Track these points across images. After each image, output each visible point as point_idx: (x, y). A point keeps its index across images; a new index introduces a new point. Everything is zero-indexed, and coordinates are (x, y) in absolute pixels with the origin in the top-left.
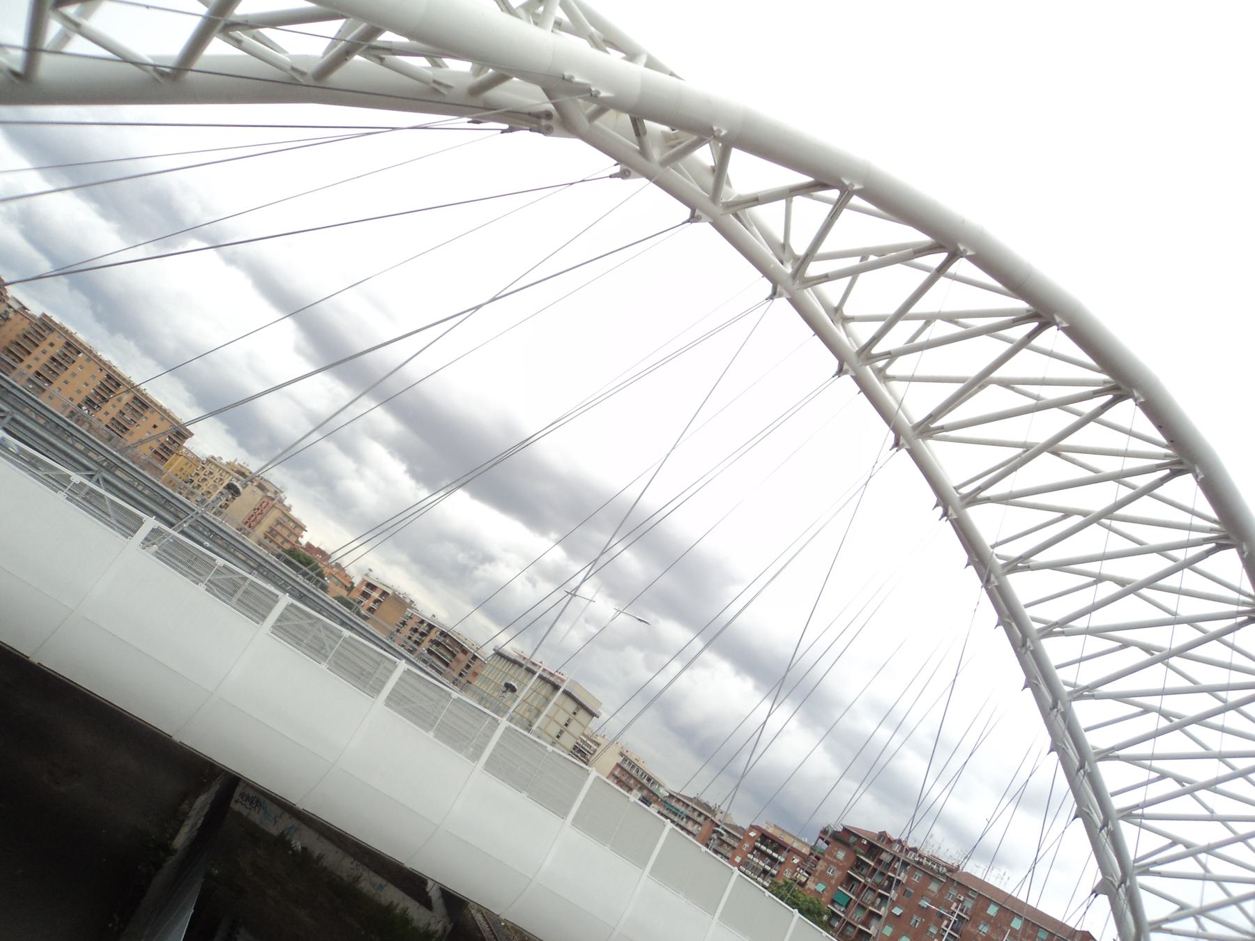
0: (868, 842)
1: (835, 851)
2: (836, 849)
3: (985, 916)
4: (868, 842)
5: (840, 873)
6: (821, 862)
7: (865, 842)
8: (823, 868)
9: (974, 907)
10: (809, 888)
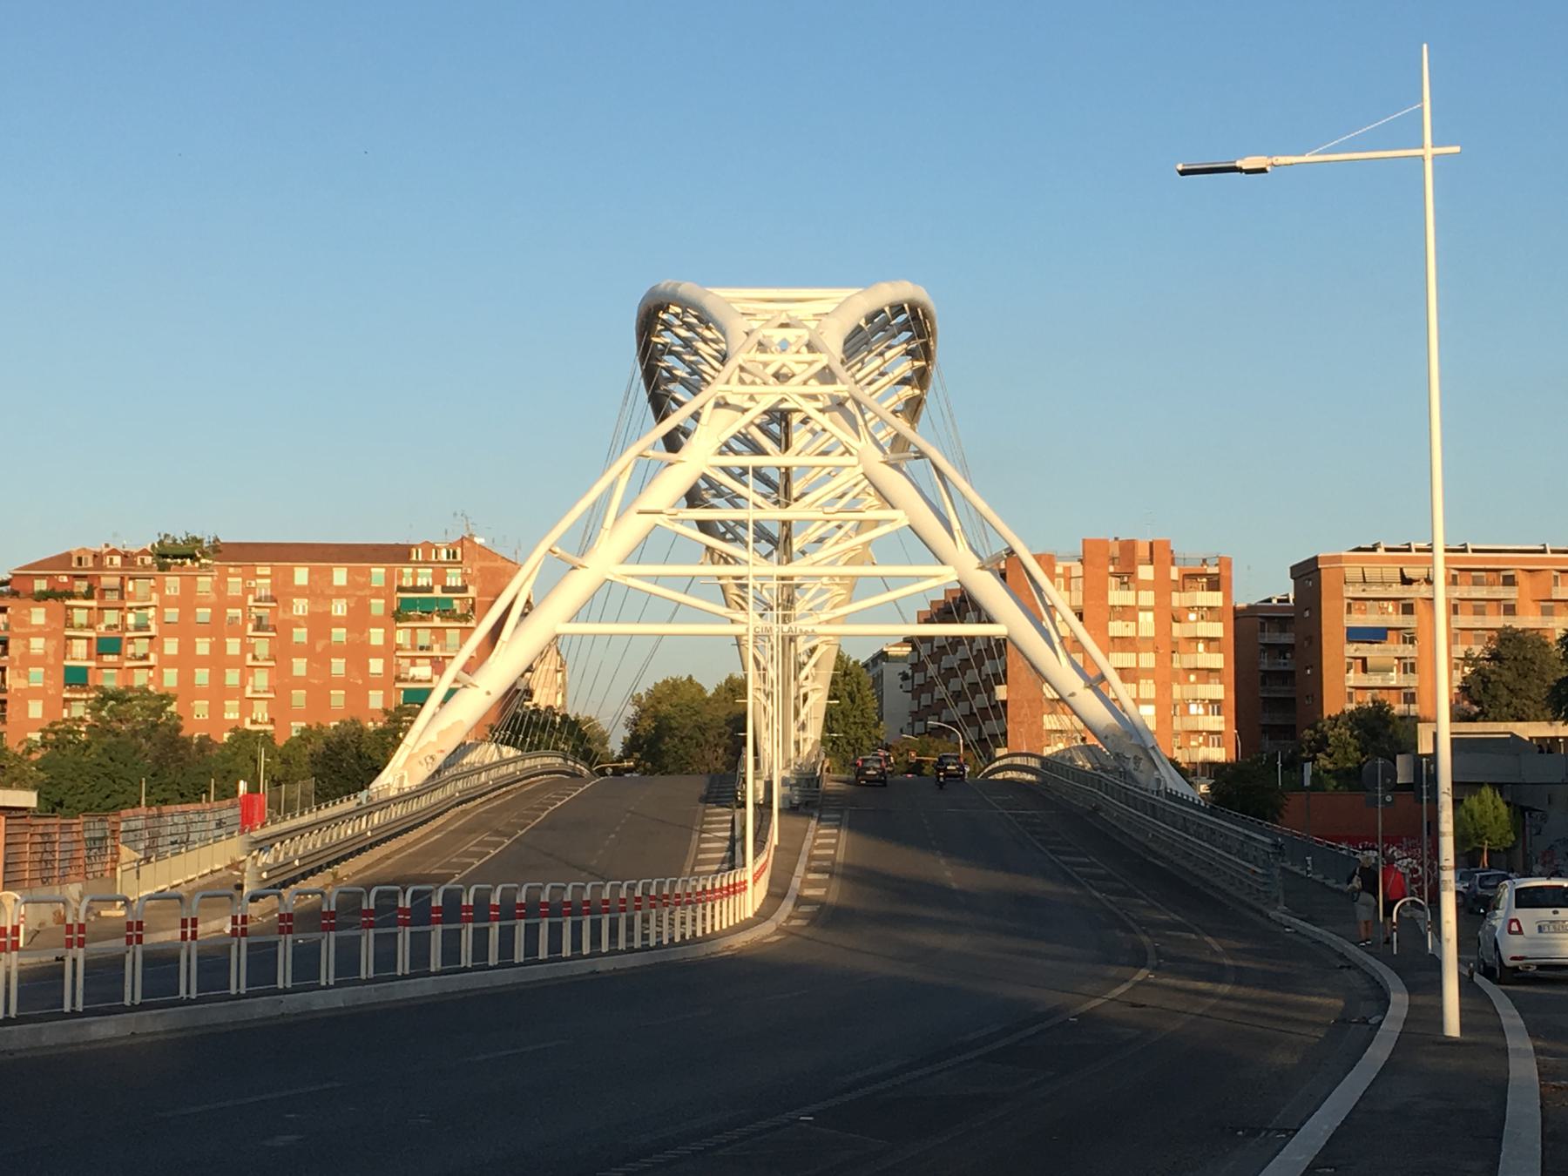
0: (68, 576)
2: (25, 612)
3: (294, 589)
4: (68, 576)
5: (54, 642)
6: (11, 643)
7: (65, 579)
8: (23, 649)
10: (16, 690)
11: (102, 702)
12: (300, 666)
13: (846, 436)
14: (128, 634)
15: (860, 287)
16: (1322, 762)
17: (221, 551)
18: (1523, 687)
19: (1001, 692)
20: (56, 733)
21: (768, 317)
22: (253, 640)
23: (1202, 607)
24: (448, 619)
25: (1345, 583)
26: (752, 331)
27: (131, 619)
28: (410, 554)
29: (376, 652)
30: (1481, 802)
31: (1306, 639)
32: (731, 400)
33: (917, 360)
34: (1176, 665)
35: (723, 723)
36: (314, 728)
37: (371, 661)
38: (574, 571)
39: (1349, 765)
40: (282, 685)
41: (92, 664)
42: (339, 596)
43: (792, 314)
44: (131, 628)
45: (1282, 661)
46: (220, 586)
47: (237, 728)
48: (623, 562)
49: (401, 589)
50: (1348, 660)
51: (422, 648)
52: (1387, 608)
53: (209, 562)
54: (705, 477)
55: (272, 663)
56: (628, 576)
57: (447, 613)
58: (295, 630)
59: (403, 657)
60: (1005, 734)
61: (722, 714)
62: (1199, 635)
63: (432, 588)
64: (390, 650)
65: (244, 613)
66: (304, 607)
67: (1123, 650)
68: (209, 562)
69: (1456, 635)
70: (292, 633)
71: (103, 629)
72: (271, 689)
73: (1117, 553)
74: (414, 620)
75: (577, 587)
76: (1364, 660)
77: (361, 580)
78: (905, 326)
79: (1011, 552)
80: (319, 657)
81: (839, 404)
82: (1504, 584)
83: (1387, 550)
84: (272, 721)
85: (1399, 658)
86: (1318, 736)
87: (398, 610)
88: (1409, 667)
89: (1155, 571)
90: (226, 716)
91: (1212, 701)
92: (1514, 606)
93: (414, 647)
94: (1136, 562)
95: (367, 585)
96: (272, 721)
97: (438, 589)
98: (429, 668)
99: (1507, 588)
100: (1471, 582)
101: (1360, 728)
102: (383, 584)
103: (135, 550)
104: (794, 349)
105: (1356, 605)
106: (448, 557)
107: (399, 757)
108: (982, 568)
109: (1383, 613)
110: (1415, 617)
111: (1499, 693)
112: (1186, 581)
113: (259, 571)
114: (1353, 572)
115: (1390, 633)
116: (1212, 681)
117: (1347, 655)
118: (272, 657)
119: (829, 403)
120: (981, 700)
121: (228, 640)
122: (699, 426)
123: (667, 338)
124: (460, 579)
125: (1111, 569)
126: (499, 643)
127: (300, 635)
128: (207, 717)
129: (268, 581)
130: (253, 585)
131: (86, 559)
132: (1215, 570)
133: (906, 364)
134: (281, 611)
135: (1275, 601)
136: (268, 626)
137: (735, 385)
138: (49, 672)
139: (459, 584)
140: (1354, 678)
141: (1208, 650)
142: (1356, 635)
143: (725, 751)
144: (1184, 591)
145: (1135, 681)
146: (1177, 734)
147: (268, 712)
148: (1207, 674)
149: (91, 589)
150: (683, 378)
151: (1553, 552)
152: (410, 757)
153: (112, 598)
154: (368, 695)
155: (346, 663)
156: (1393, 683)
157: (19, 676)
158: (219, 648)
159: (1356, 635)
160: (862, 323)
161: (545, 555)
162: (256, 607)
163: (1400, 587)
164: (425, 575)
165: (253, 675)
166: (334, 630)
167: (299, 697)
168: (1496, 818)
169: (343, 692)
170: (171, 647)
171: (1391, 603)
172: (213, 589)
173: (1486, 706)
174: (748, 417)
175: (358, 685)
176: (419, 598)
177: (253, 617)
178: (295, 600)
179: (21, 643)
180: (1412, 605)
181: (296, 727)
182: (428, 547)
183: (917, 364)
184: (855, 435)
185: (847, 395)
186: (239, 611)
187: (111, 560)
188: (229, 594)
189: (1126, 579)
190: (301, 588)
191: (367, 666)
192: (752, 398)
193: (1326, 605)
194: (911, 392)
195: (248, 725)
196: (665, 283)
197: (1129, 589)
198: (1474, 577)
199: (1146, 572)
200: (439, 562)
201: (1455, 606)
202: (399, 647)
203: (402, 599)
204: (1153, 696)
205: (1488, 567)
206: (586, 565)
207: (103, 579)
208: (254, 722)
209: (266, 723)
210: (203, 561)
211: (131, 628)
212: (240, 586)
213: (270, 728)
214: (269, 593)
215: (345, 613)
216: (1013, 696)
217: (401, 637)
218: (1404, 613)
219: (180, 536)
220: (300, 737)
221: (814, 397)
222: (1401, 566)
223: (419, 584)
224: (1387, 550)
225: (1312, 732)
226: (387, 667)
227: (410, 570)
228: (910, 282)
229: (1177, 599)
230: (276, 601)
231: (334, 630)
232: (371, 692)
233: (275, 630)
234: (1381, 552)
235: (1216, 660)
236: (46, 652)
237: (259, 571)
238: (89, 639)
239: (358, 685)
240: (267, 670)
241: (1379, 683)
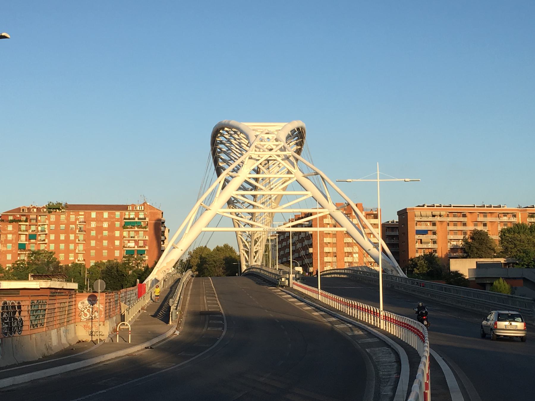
0: (20, 215)
1: (6, 227)
2: (6, 226)
4: (20, 215)
5: (15, 236)
7: (19, 216)
8: (5, 238)
9: (85, 218)
10: (3, 251)
11: (32, 254)
12: (93, 243)
13: (291, 168)
14: (39, 233)
15: (287, 122)
16: (416, 271)
17: (69, 207)
18: (481, 248)
19: (311, 250)
20: (17, 264)
21: (261, 131)
22: (78, 235)
24: (140, 228)
26: (258, 135)
27: (40, 228)
28: (127, 208)
29: (117, 239)
30: (499, 283)
31: (403, 233)
32: (252, 157)
35: (222, 260)
36: (99, 262)
37: (116, 241)
38: (207, 211)
39: (424, 272)
40: (87, 249)
41: (27, 243)
42: (105, 221)
43: (269, 130)
44: (40, 231)
45: (393, 240)
46: (68, 218)
47: (74, 262)
48: (221, 208)
49: (125, 219)
50: (416, 240)
51: (132, 237)
53: (64, 210)
54: (246, 181)
55: (84, 242)
56: (224, 212)
57: (140, 226)
58: (92, 232)
59: (125, 240)
60: (312, 263)
61: (222, 257)
63: (135, 218)
64: (122, 237)
65: (75, 226)
66: (94, 225)
68: (64, 210)
69: (449, 232)
70: (90, 233)
71: (31, 232)
72: (84, 250)
74: (129, 229)
75: (208, 216)
76: (421, 240)
77: (112, 216)
78: (297, 136)
79: (349, 204)
80: (100, 241)
81: (287, 158)
83: (427, 206)
84: (84, 260)
85: (431, 239)
86: (414, 263)
87: (124, 225)
88: (435, 242)
90: (70, 259)
92: (486, 223)
93: (129, 237)
95: (114, 217)
96: (84, 260)
97: (136, 219)
98: (134, 244)
100: (453, 215)
101: (427, 261)
102: (119, 217)
103: (41, 207)
104: (272, 141)
105: (418, 223)
106: (140, 209)
107: (154, 271)
108: (338, 209)
109: (427, 226)
110: (436, 227)
111: (474, 250)
113: (80, 213)
114: (417, 213)
115: (429, 232)
117: (416, 238)
118: (84, 240)
119: (284, 158)
121: (70, 235)
122: (244, 165)
123: (221, 138)
124: (143, 216)
126: (185, 234)
127: (93, 233)
128: (64, 259)
129: (83, 216)
130: (78, 217)
131: (25, 210)
133: (295, 147)
134: (87, 226)
135: (390, 222)
136: (83, 230)
137: (254, 152)
138: (13, 245)
139: (143, 217)
140: (418, 245)
142: (419, 232)
143: (222, 269)
145: (352, 246)
147: (83, 257)
149: (27, 219)
150: (224, 151)
151: (477, 207)
152: (158, 271)
153: (34, 222)
154: (115, 252)
155: (108, 242)
156: (430, 247)
157: (4, 246)
158: (67, 237)
159: (419, 232)
160: (290, 133)
161: (200, 205)
162: (80, 225)
163: (431, 218)
164: (132, 214)
165: (78, 246)
166: (104, 232)
167: (93, 252)
168: (505, 289)
169: (107, 251)
170: (52, 237)
171: (429, 222)
172: (65, 218)
173: (470, 254)
174: (259, 162)
175: (111, 249)
176: (131, 222)
177: (78, 228)
178: (91, 222)
179: (4, 236)
180: (435, 223)
181: (92, 263)
182: (133, 206)
184: (293, 168)
185: (291, 155)
186: (74, 226)
187: (33, 210)
188: (71, 220)
189: (349, 215)
190: (94, 218)
191: (115, 242)
192: (259, 156)
195: (77, 261)
196: (225, 121)
198: (454, 214)
200: (137, 210)
201: (448, 223)
202: (124, 237)
203: (125, 222)
204: (357, 251)
205: (458, 211)
206: (211, 209)
207: (30, 216)
208: (78, 261)
209: (83, 261)
210: (62, 210)
211: (40, 231)
212: (74, 218)
213: (84, 262)
214: (83, 220)
215: (107, 226)
216: (315, 251)
217: (125, 234)
218: (433, 225)
219: (55, 202)
220: (95, 265)
221: (279, 156)
223: (131, 217)
224: (427, 206)
225: (412, 262)
226: (120, 243)
227: (128, 213)
228: (302, 121)
230: (85, 223)
231: (104, 232)
232: (115, 251)
233: (85, 232)
234: (425, 207)
236: (12, 239)
237: (80, 213)
238: (26, 235)
239: (111, 249)
240: (83, 244)
241: (426, 247)
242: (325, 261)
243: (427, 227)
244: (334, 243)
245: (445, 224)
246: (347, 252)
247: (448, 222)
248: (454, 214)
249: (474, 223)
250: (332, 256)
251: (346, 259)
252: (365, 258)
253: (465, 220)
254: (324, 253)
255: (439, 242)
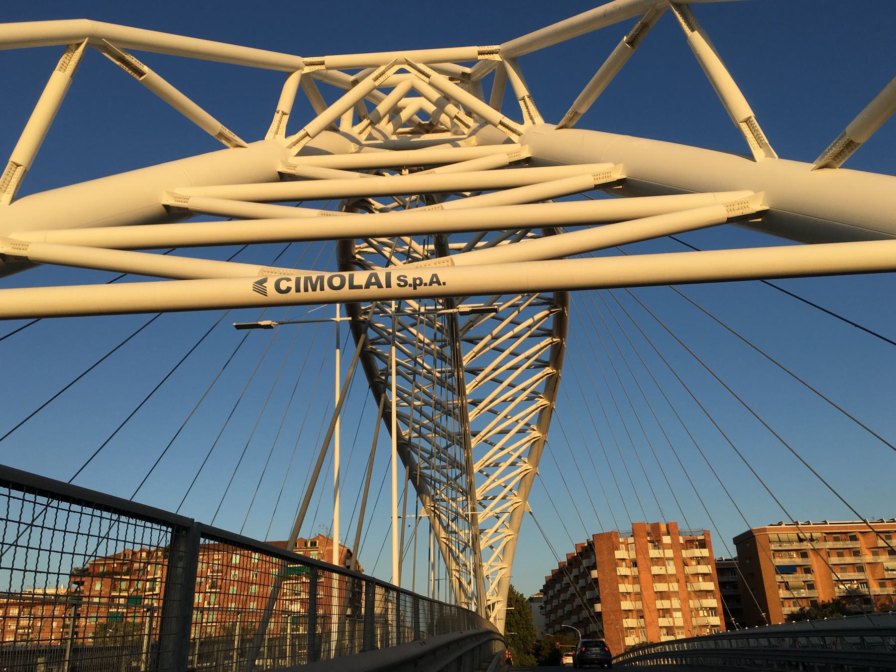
23: (698, 557)
25: (770, 542)
33: (555, 338)
34: (689, 589)
45: (725, 590)
52: (793, 555)
62: (700, 572)
67: (660, 582)
73: (650, 531)
82: (851, 540)
83: (786, 525)
85: (804, 582)
88: (811, 586)
89: (672, 538)
91: (711, 609)
94: (661, 535)
99: (854, 542)
100: (832, 539)
105: (777, 554)
109: (791, 558)
110: (810, 559)
112: (687, 544)
114: (773, 536)
116: (709, 597)
120: (585, 614)
125: (649, 538)
132: (702, 537)
140: (783, 593)
141: (704, 580)
144: (687, 549)
145: (669, 598)
146: (694, 628)
148: (706, 593)
156: (804, 595)
183: (555, 340)
193: (762, 555)
194: (552, 371)
197: (659, 549)
198: (834, 537)
199: (666, 540)
205: (842, 531)
222: (797, 532)
224: (786, 525)
229: (685, 554)
234: (783, 526)
235: (710, 586)
242: (625, 625)
243: (793, 559)
244: (637, 594)
245: (823, 554)
246: (662, 609)
247: (828, 550)
248: (836, 536)
249: (872, 550)
250: (636, 617)
251: (663, 622)
252: (694, 619)
253: (858, 546)
254: (623, 613)
255: (819, 585)
